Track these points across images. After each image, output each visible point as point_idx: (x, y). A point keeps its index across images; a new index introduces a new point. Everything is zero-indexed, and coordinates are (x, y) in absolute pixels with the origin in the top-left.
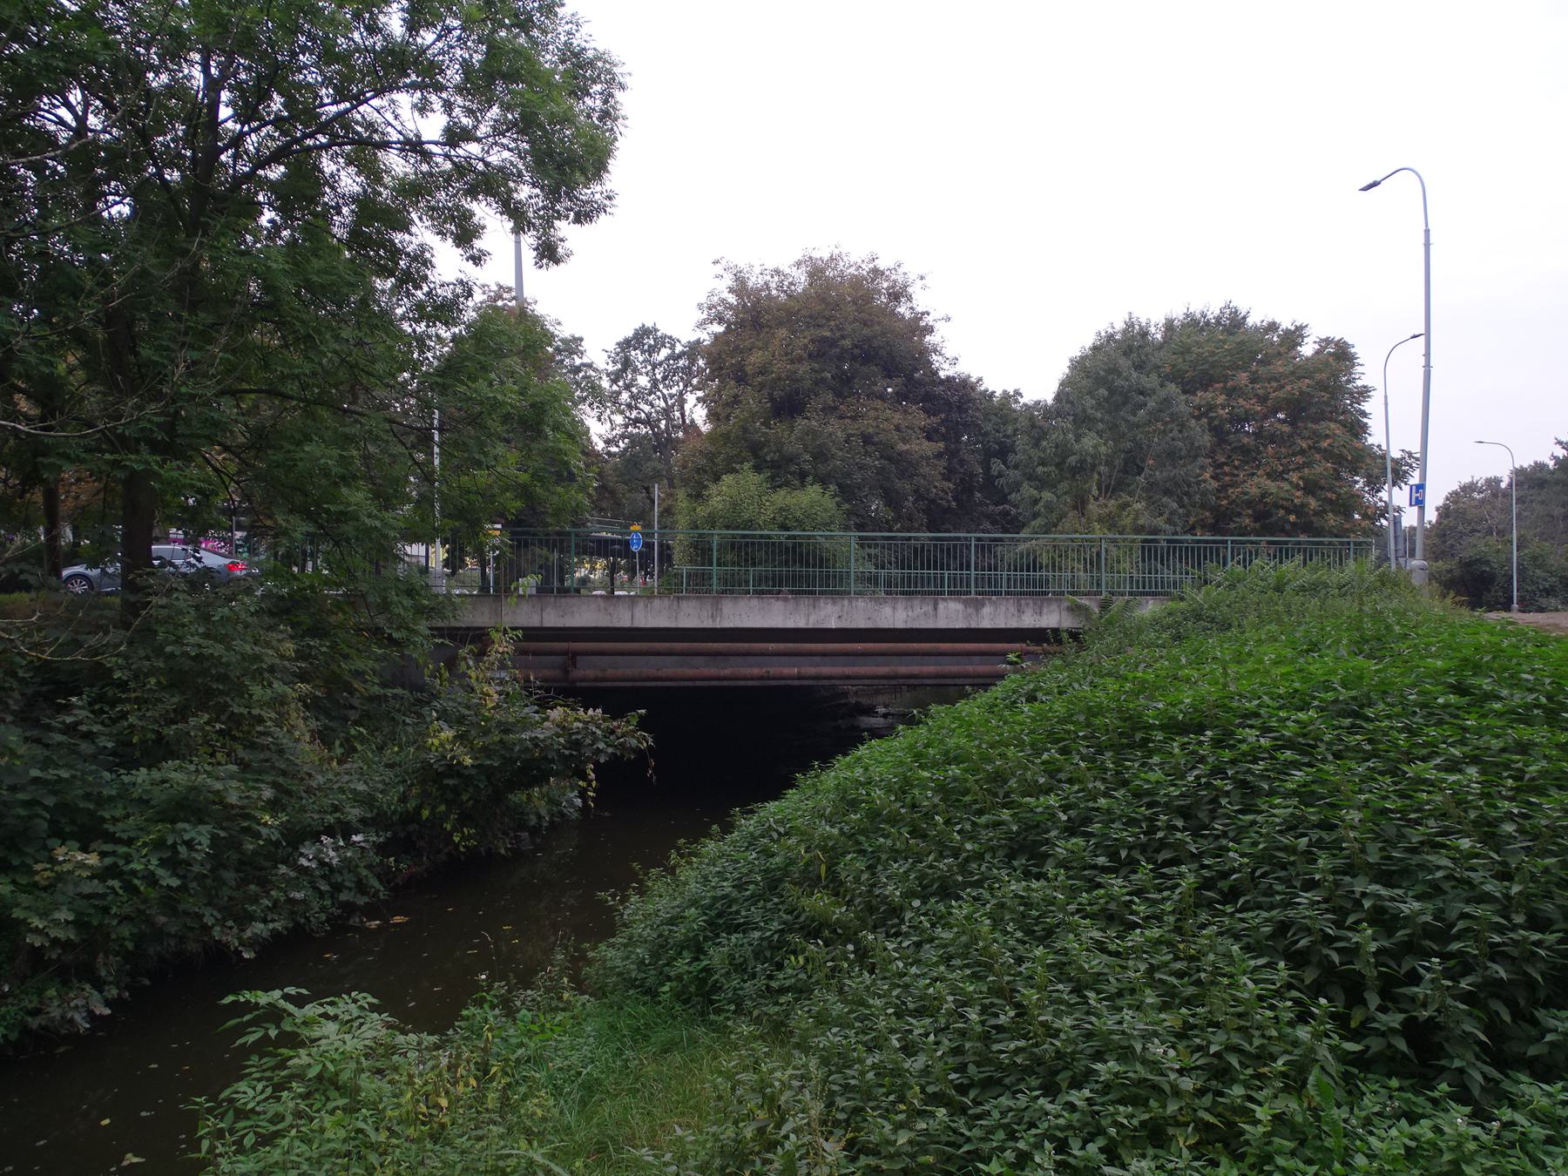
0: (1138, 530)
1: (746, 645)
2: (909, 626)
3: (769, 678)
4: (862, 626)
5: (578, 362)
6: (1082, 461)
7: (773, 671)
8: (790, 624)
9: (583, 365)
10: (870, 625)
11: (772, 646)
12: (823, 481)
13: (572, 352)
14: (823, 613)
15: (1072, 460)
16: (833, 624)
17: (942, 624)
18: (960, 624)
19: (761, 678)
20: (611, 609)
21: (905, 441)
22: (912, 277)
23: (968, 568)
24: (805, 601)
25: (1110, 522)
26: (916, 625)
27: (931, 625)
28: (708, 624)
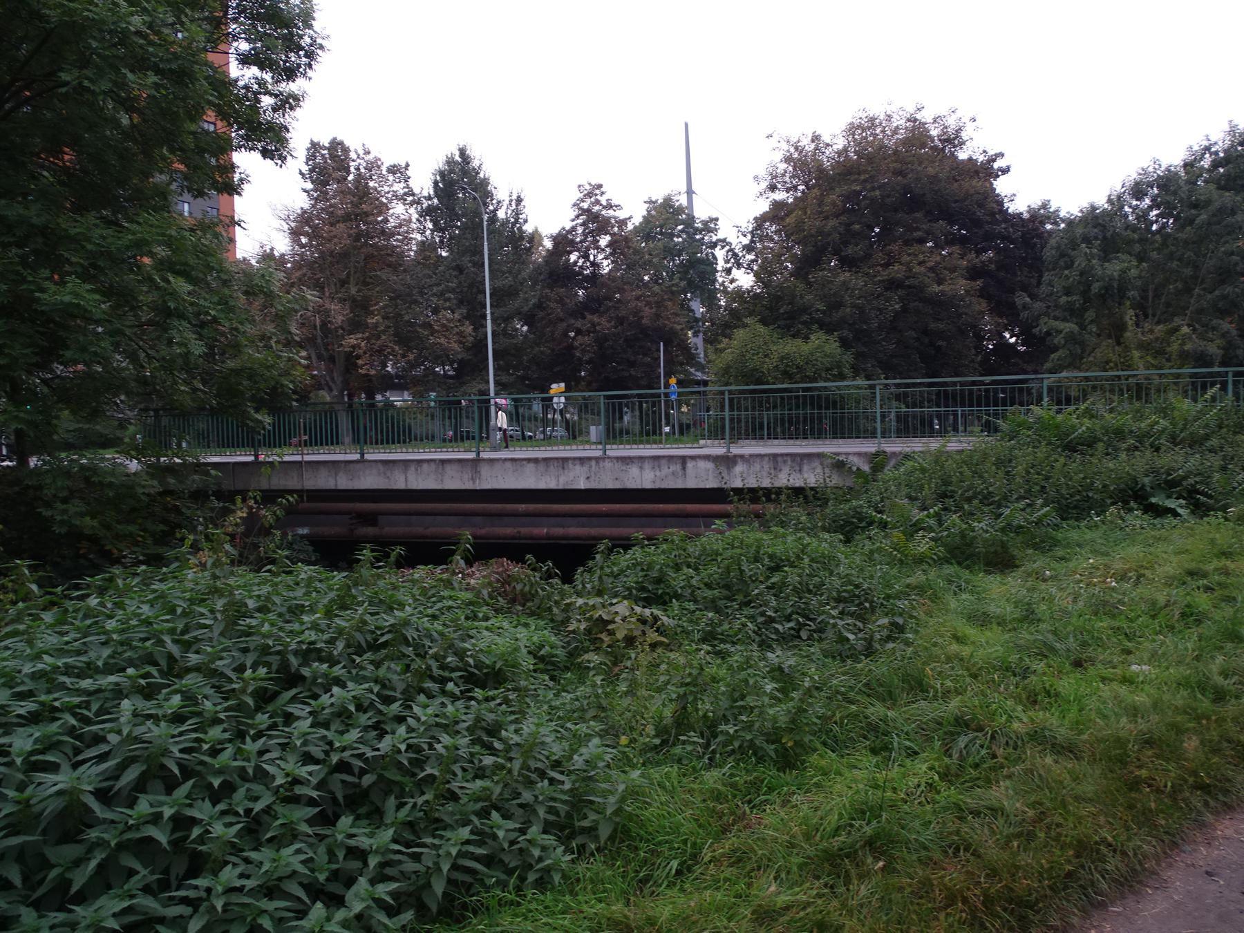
0: (1184, 357)
1: (540, 506)
2: (658, 485)
3: (520, 538)
4: (610, 486)
5: (714, 239)
6: (1107, 288)
7: (524, 531)
8: (542, 485)
9: (720, 240)
10: (618, 486)
11: (522, 507)
12: (828, 328)
13: (710, 231)
14: (571, 474)
15: (1096, 287)
16: (582, 484)
17: (691, 484)
18: (712, 484)
19: (513, 538)
20: (389, 474)
21: (940, 282)
22: (966, 119)
23: (732, 420)
24: (820, 442)
25: (1157, 351)
26: (664, 485)
27: (679, 484)
28: (469, 485)
